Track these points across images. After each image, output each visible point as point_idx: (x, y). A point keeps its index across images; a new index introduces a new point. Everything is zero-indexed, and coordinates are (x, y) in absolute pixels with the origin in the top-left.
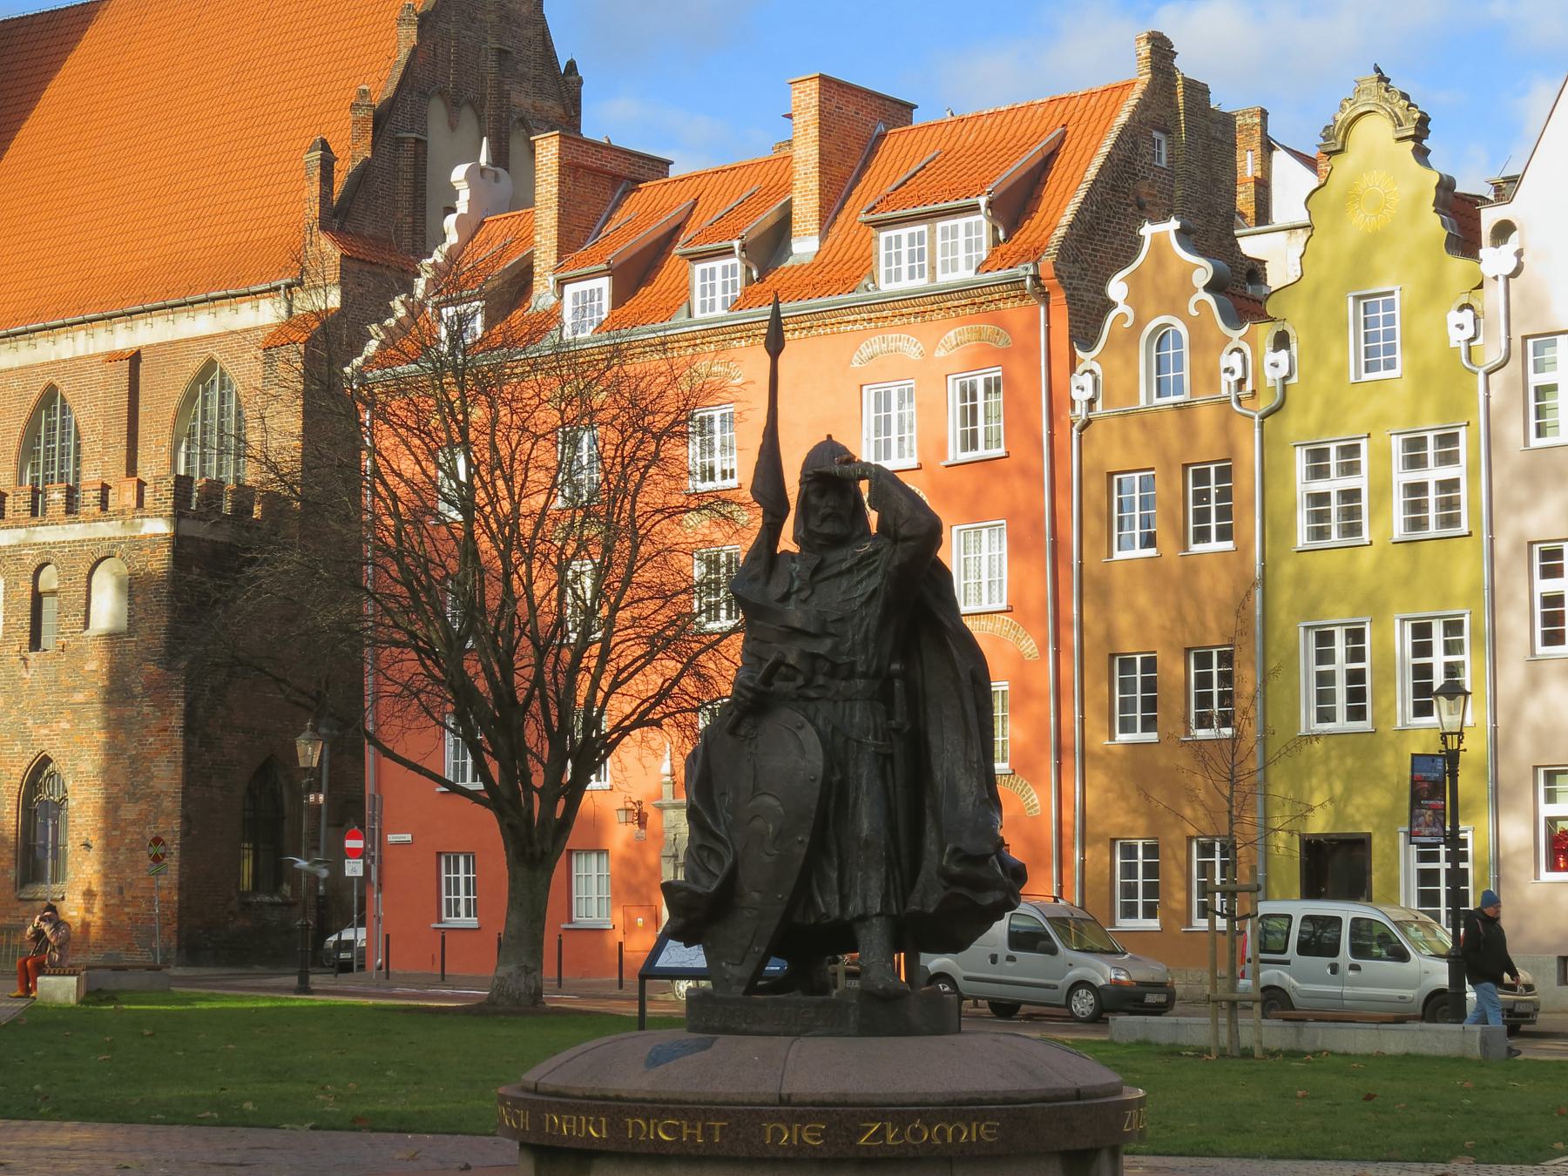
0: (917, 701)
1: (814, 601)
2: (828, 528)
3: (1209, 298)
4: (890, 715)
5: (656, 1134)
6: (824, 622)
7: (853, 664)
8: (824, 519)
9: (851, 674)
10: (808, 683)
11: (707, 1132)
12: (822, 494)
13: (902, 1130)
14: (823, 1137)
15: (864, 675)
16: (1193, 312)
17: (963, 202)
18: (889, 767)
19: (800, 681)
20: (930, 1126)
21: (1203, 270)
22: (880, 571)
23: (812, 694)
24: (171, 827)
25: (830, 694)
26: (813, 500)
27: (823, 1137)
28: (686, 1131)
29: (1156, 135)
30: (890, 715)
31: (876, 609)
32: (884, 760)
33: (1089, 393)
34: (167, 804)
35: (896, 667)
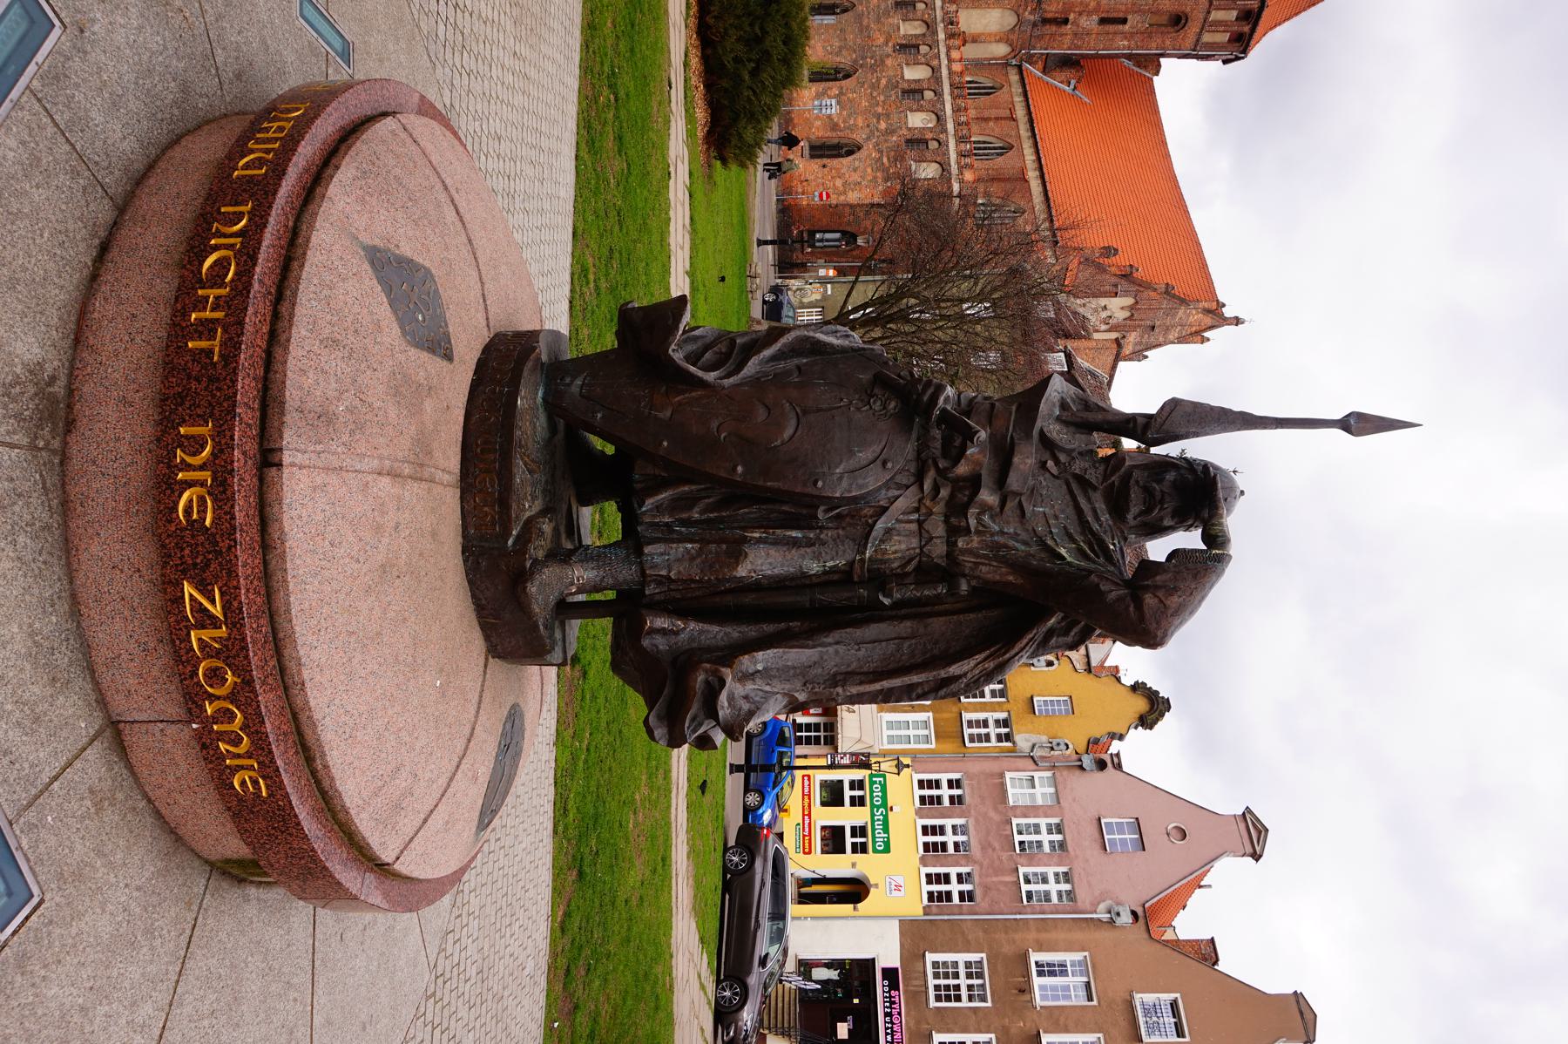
5: (216, 248)
9: (954, 532)
11: (206, 329)
13: (218, 654)
14: (191, 522)
20: (232, 697)
24: (834, 200)
26: (1170, 476)
27: (191, 522)
28: (212, 294)
34: (842, 198)
35: (964, 587)
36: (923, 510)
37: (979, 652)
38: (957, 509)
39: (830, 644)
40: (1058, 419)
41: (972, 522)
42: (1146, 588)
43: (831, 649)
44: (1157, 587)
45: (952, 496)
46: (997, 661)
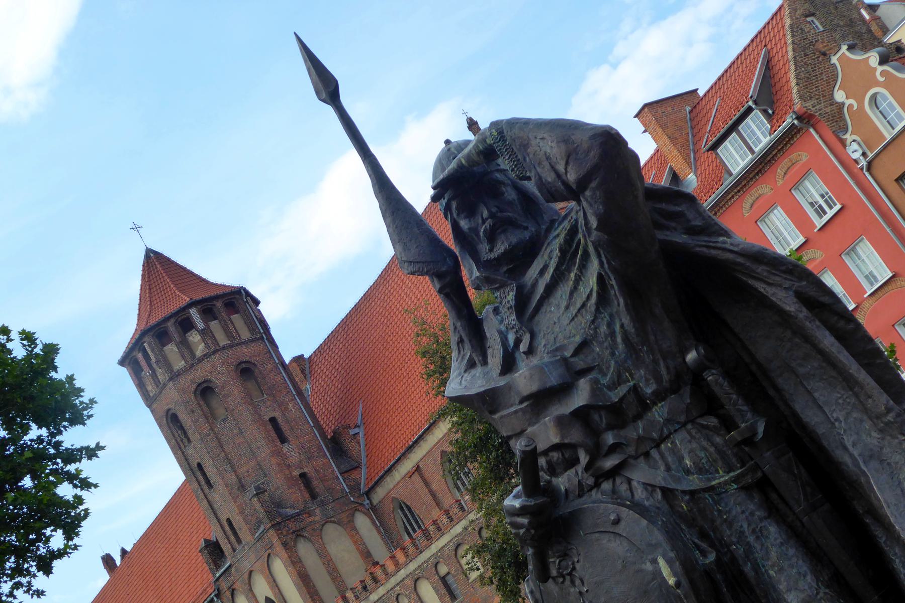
0: (758, 387)
1: (541, 342)
2: (501, 247)
3: (886, 67)
4: (728, 424)
6: (565, 360)
7: (635, 389)
8: (492, 238)
9: (644, 405)
10: (596, 453)
12: (470, 211)
15: (660, 396)
16: (881, 79)
17: (742, 110)
18: (774, 496)
19: (584, 458)
21: (873, 58)
22: (591, 249)
23: (609, 463)
25: (631, 450)
29: (809, 19)
30: (728, 424)
31: (619, 302)
32: (762, 488)
33: (860, 152)
36: (643, 449)
37: (756, 289)
38: (619, 415)
39: (851, 456)
40: (485, 363)
41: (622, 390)
42: (565, 184)
43: (856, 453)
44: (558, 175)
45: (610, 427)
46: (754, 267)
